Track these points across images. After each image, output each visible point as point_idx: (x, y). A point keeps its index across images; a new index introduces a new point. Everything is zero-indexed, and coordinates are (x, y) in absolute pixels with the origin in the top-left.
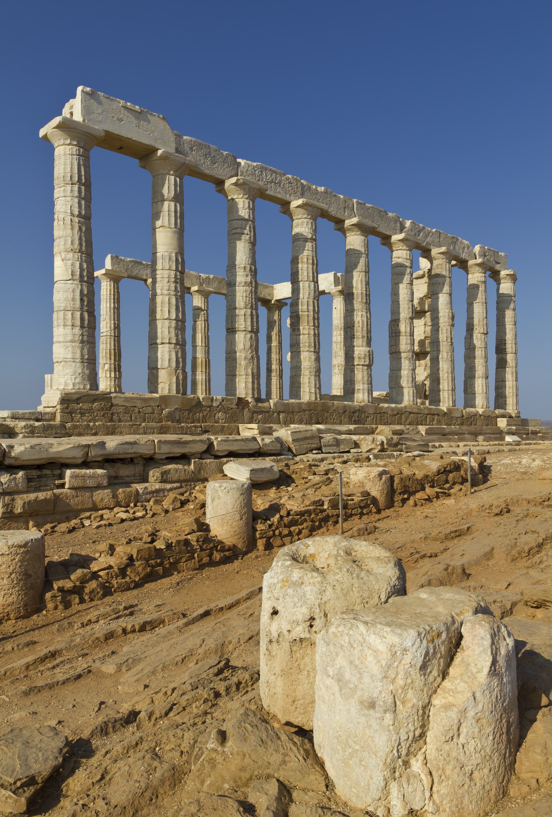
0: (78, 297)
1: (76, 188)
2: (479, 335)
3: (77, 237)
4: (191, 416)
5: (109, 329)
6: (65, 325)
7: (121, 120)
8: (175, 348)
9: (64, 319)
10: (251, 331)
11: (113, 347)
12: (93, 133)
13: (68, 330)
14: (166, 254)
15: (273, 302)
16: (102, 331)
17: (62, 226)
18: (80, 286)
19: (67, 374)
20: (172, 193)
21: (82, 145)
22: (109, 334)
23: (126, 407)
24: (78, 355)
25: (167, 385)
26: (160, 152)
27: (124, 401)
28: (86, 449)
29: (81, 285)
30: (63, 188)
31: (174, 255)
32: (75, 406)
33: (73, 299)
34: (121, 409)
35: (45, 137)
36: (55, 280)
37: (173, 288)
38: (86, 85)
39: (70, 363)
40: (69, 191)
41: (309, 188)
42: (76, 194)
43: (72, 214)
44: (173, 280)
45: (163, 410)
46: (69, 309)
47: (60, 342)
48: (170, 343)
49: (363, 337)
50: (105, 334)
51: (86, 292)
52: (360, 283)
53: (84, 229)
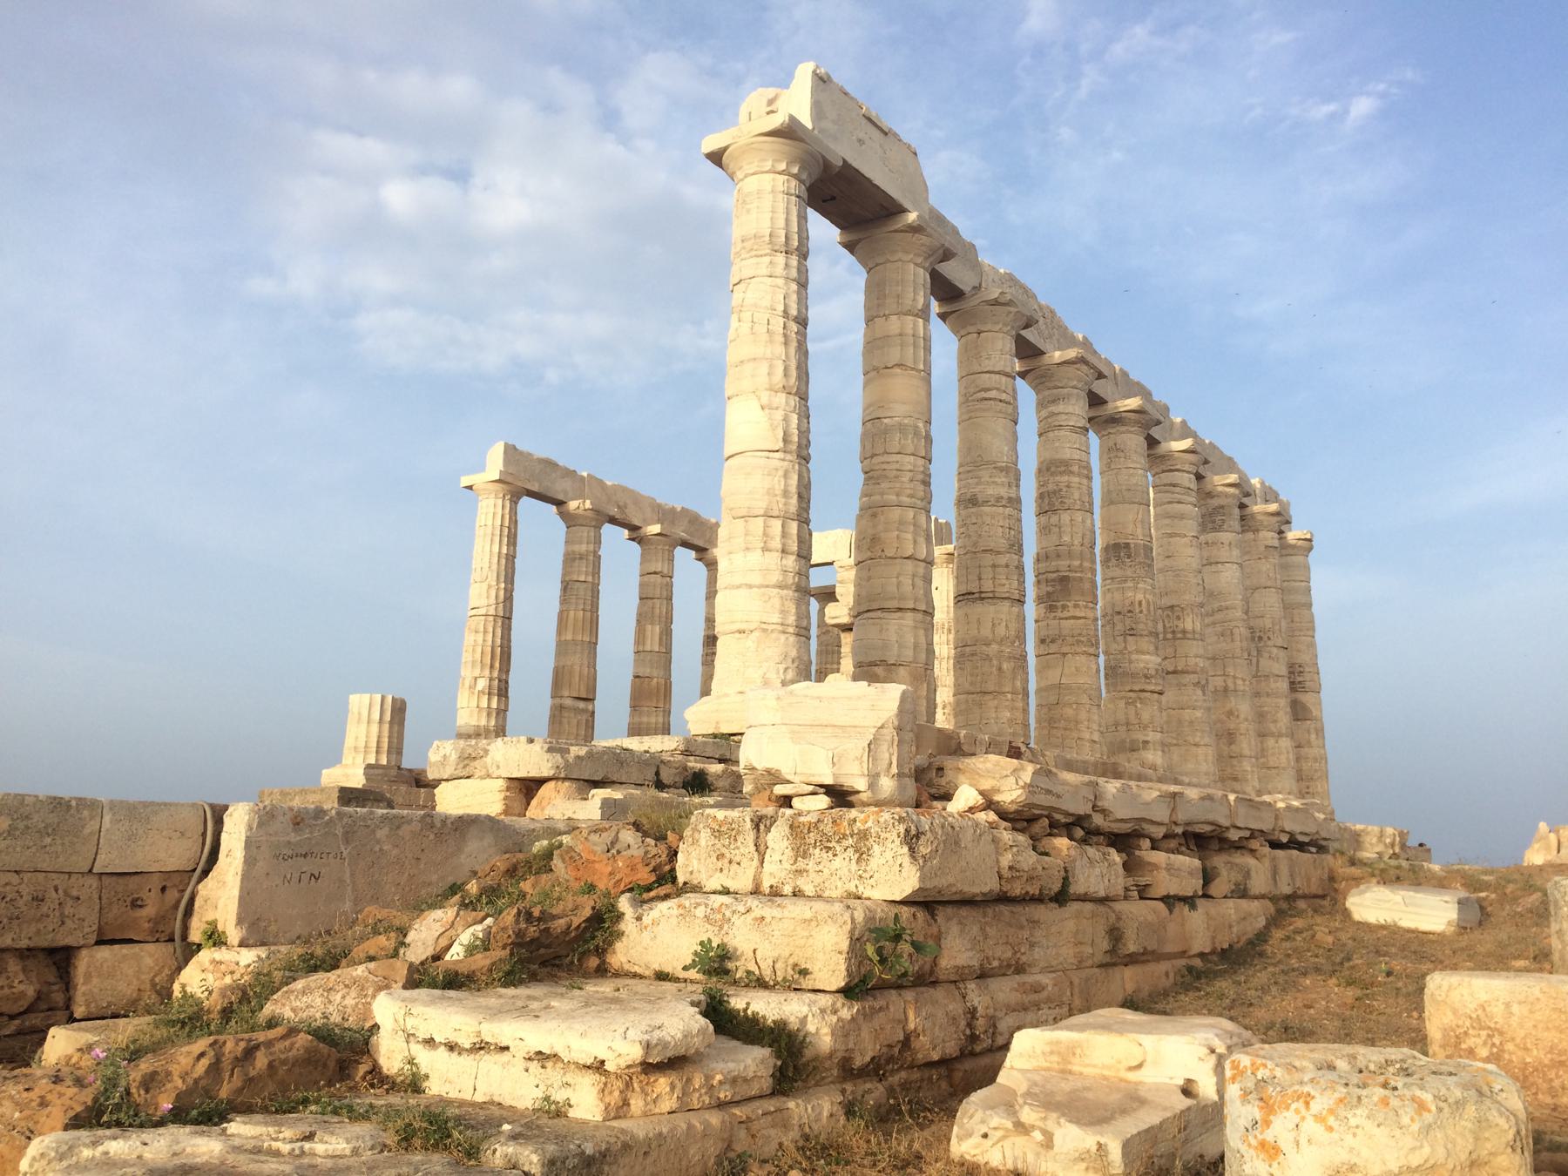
0: (793, 489)
2: (1275, 650)
6: (765, 549)
9: (765, 534)
13: (773, 559)
17: (765, 337)
21: (804, 177)
22: (492, 612)
24: (792, 619)
26: (912, 217)
30: (767, 259)
33: (786, 493)
39: (774, 635)
43: (786, 313)
46: (776, 513)
47: (750, 587)
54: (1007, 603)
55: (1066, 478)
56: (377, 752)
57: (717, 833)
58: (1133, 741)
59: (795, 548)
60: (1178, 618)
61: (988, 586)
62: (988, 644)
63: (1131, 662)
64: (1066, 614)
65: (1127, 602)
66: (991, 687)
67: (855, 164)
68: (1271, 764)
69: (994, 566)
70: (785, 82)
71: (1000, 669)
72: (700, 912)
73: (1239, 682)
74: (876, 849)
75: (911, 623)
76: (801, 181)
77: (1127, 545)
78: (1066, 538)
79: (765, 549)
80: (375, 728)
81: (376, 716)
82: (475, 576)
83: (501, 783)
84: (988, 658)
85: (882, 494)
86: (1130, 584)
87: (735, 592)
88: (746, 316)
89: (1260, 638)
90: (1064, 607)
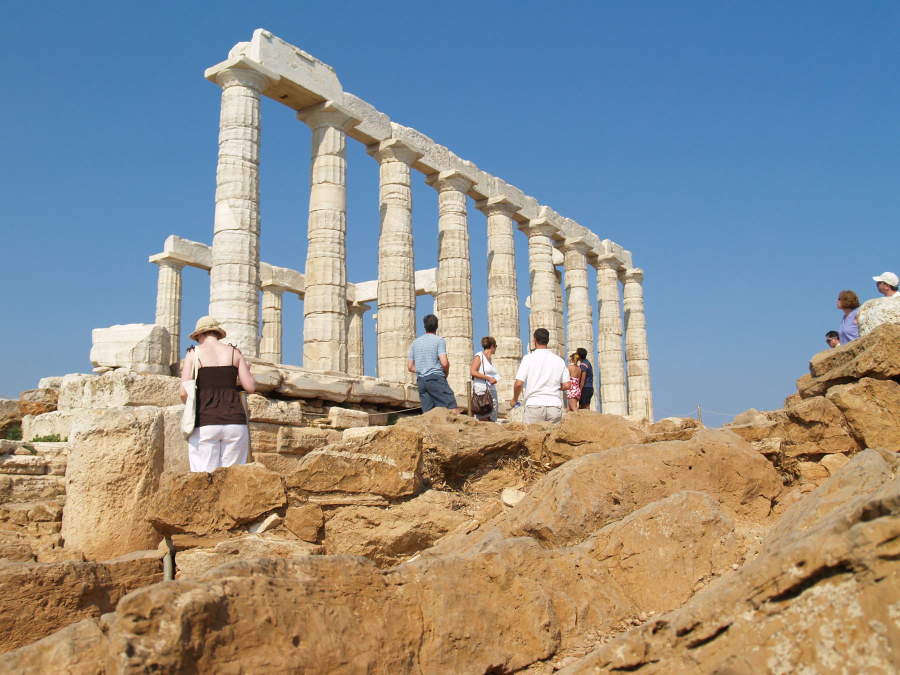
0: (247, 249)
2: (614, 336)
3: (248, 182)
7: (294, 67)
10: (410, 307)
12: (270, 76)
14: (329, 211)
15: (354, 304)
24: (245, 316)
28: (350, 386)
33: (242, 252)
35: (214, 78)
36: (216, 230)
37: (337, 250)
41: (455, 160)
42: (249, 137)
47: (223, 300)
48: (332, 312)
49: (512, 326)
51: (255, 245)
57: (71, 389)
65: (500, 309)
66: (393, 354)
67: (290, 78)
70: (249, 38)
72: (47, 418)
74: (115, 388)
75: (330, 319)
78: (452, 274)
82: (158, 312)
84: (392, 339)
90: (451, 311)
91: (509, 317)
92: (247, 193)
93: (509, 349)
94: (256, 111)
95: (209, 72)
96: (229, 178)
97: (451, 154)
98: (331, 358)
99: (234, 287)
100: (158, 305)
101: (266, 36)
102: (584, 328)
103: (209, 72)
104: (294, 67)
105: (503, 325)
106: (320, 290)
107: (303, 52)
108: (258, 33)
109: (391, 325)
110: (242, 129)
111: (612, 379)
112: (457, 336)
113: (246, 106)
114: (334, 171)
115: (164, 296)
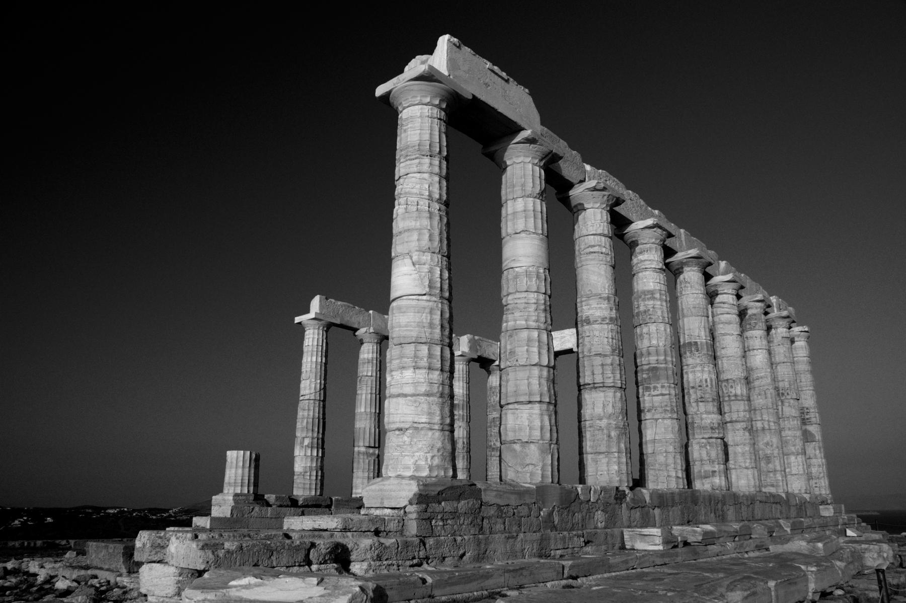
1: (436, 162)
2: (792, 401)
3: (436, 232)
4: (570, 517)
5: (313, 391)
8: (548, 410)
11: (317, 415)
16: (302, 393)
18: (440, 305)
19: (419, 450)
20: (538, 190)
23: (499, 506)
24: (437, 419)
25: (539, 468)
27: (496, 496)
29: (442, 303)
30: (417, 161)
31: (542, 271)
32: (434, 507)
33: (431, 325)
34: (492, 511)
35: (386, 97)
36: (393, 295)
37: (543, 319)
38: (453, 35)
39: (423, 432)
40: (428, 165)
42: (437, 170)
44: (543, 307)
45: (540, 509)
47: (405, 396)
48: (540, 402)
49: (714, 400)
50: (307, 397)
52: (703, 330)
53: (445, 220)
54: (612, 390)
55: (651, 302)
56: (242, 486)
58: (705, 471)
59: (438, 365)
60: (732, 387)
61: (598, 379)
62: (600, 419)
63: (702, 419)
64: (656, 393)
65: (698, 381)
66: (603, 449)
68: (793, 472)
69: (602, 365)
71: (609, 436)
73: (772, 424)
76: (441, 109)
77: (696, 343)
78: (654, 342)
79: (416, 368)
80: (240, 471)
81: (241, 464)
82: (303, 376)
83: (172, 570)
84: (601, 429)
85: (515, 320)
86: (699, 368)
87: (394, 400)
88: (402, 200)
89: (783, 394)
90: (655, 388)
91: (708, 389)
92: (436, 243)
93: (712, 428)
94: (444, 136)
95: (380, 91)
96: (412, 224)
97: (642, 202)
98: (541, 464)
99: (422, 375)
100: (304, 369)
101: (455, 44)
102: (769, 396)
103: (380, 91)
104: (487, 85)
105: (702, 400)
106: (522, 374)
107: (496, 68)
108: (444, 41)
109: (599, 410)
110: (427, 160)
111: (793, 449)
112: (664, 419)
113: (432, 129)
114: (535, 218)
115: (309, 359)
